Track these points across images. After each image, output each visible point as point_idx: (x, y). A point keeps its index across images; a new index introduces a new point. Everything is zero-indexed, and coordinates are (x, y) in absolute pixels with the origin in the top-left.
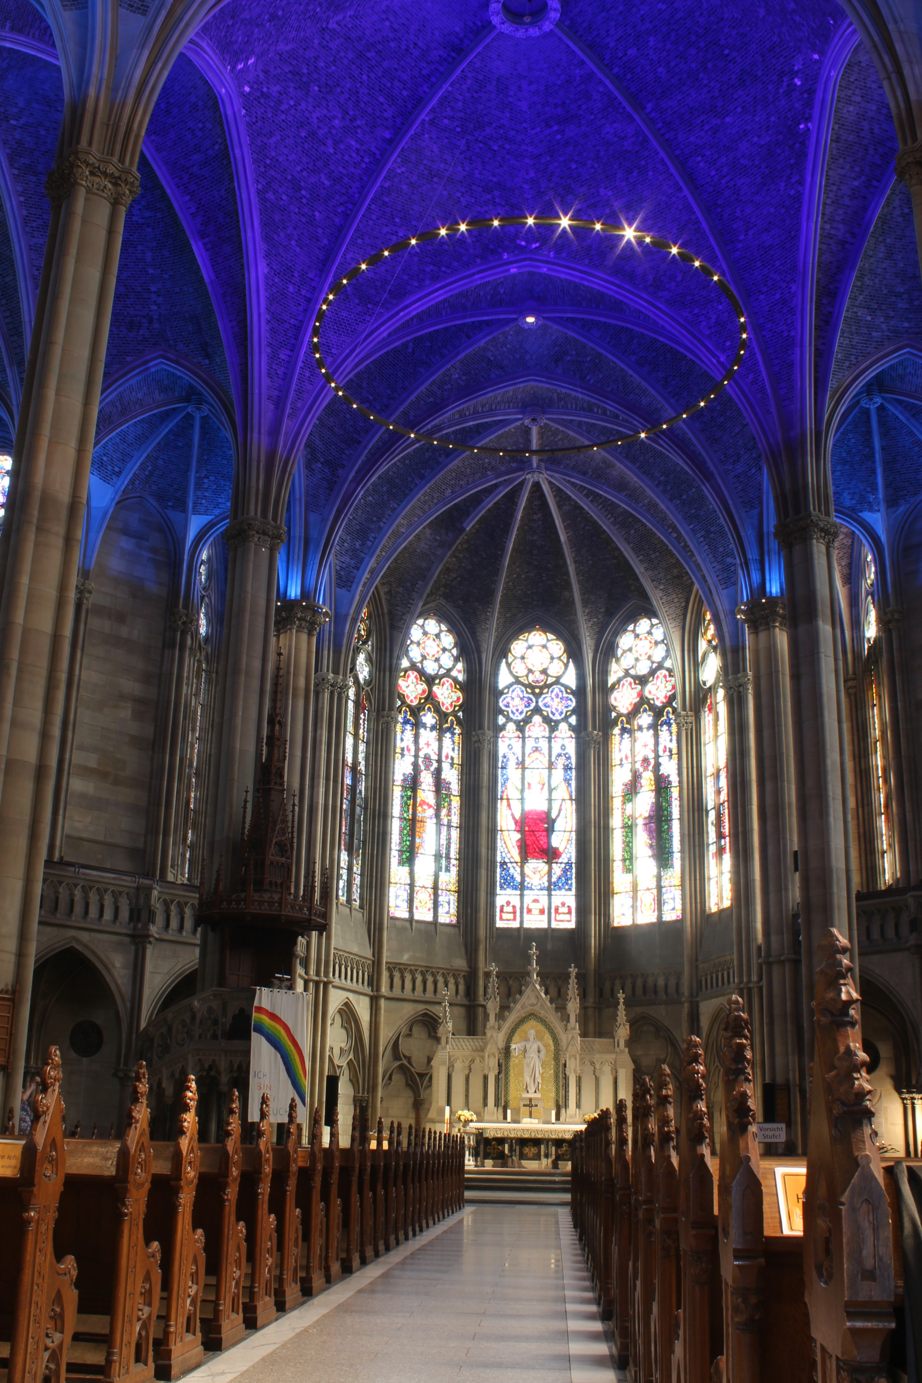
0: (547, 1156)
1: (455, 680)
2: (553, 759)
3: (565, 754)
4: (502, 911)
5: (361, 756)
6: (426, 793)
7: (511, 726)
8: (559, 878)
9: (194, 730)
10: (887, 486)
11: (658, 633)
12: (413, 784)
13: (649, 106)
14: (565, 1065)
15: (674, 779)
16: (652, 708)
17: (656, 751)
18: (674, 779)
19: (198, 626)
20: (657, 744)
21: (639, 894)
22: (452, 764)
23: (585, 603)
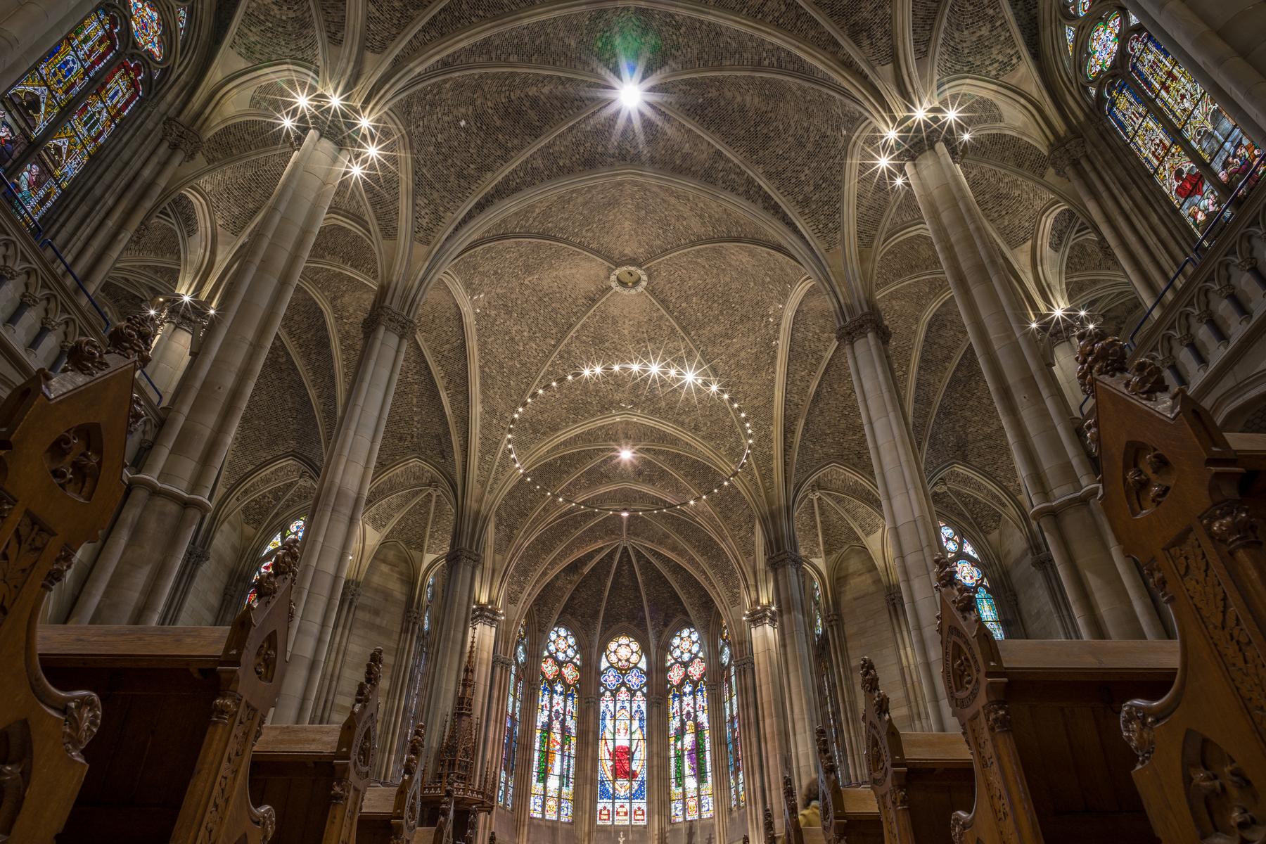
1: (575, 664)
5: (517, 709)
6: (556, 736)
7: (608, 693)
9: (415, 688)
10: (825, 543)
11: (695, 637)
12: (547, 728)
13: (693, 333)
15: (706, 725)
16: (692, 681)
17: (694, 708)
18: (706, 725)
19: (423, 624)
20: (695, 704)
23: (652, 619)
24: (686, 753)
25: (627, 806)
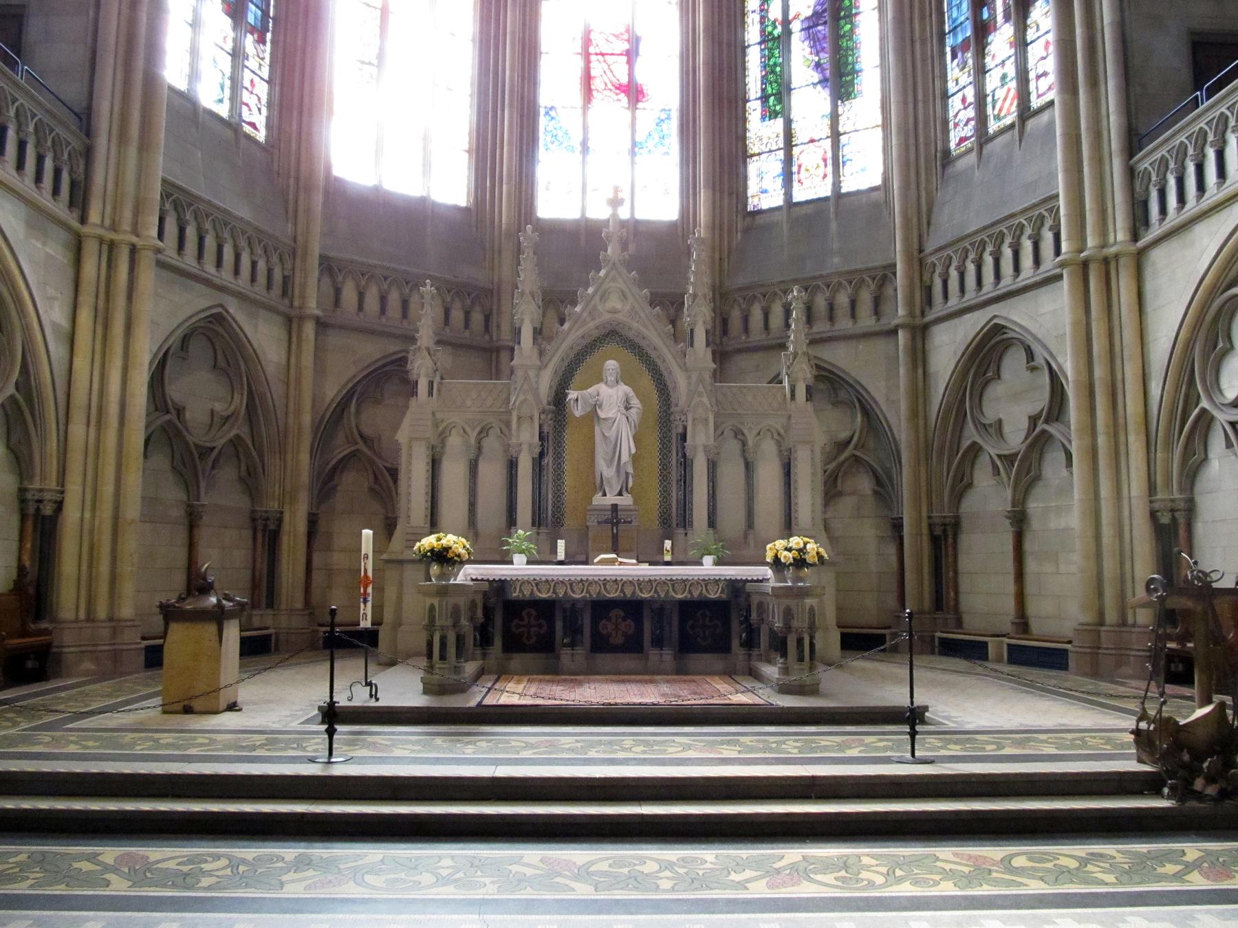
0: (658, 642)
14: (684, 437)
21: (795, 151)
24: (796, 26)
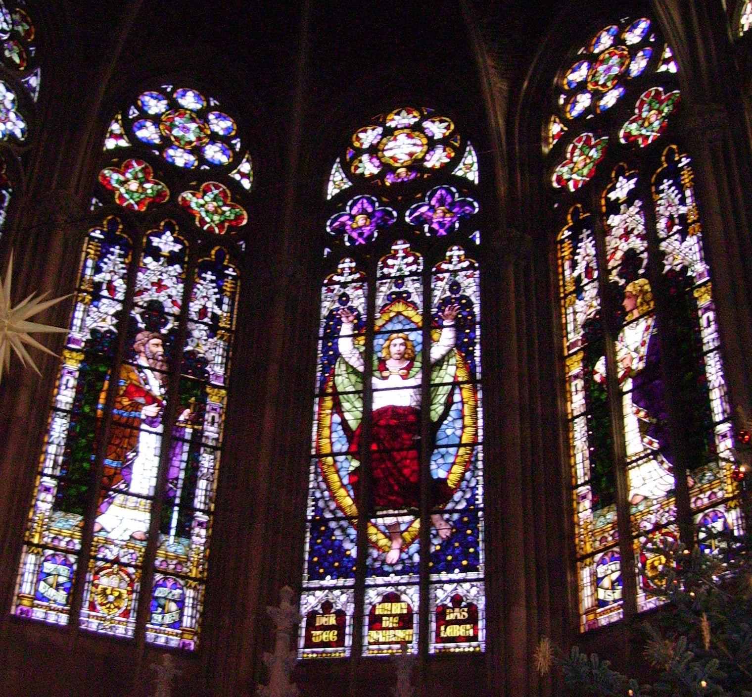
1: (235, 186)
2: (434, 310)
3: (458, 300)
4: (311, 626)
7: (347, 264)
8: (447, 544)
17: (651, 236)
22: (213, 330)
25: (412, 597)
